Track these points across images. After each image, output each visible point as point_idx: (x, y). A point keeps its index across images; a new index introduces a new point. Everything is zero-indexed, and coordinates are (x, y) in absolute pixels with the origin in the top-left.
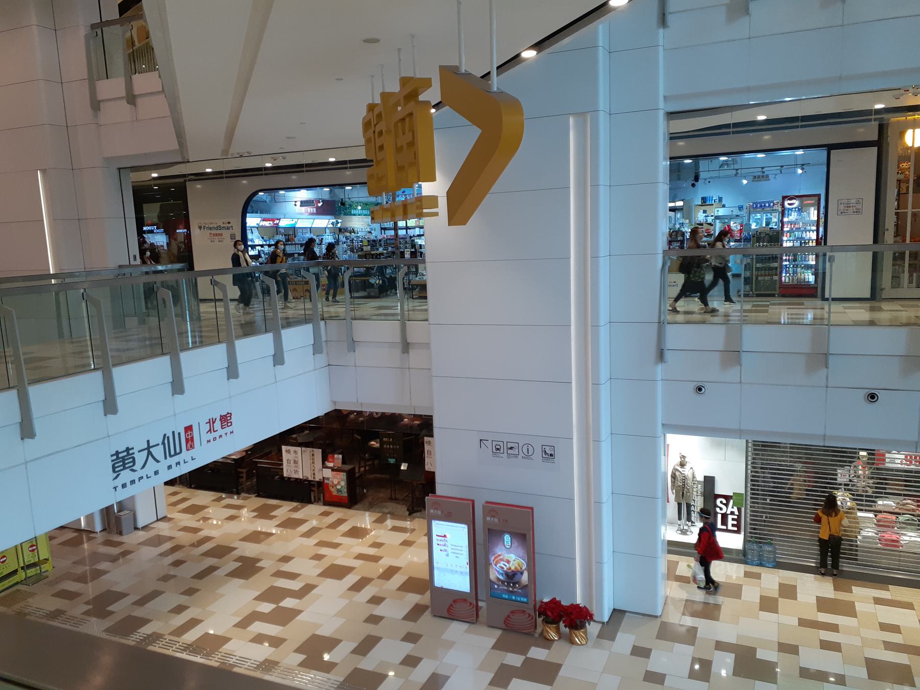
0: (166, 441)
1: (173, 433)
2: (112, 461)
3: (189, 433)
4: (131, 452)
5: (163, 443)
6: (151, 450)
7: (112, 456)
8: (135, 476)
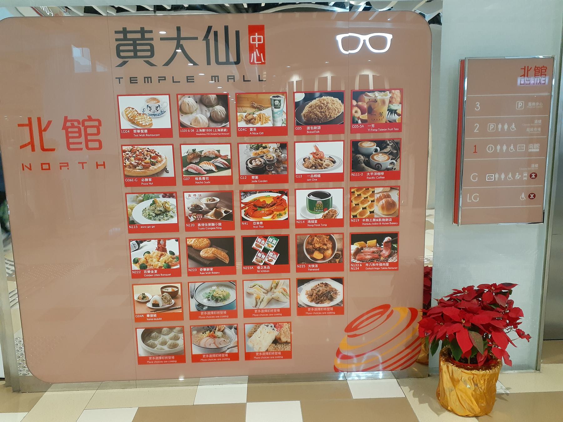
0: (211, 36)
1: (226, 28)
2: (117, 40)
3: (257, 36)
4: (147, 36)
5: (206, 37)
6: (182, 42)
7: (116, 32)
8: (154, 73)
